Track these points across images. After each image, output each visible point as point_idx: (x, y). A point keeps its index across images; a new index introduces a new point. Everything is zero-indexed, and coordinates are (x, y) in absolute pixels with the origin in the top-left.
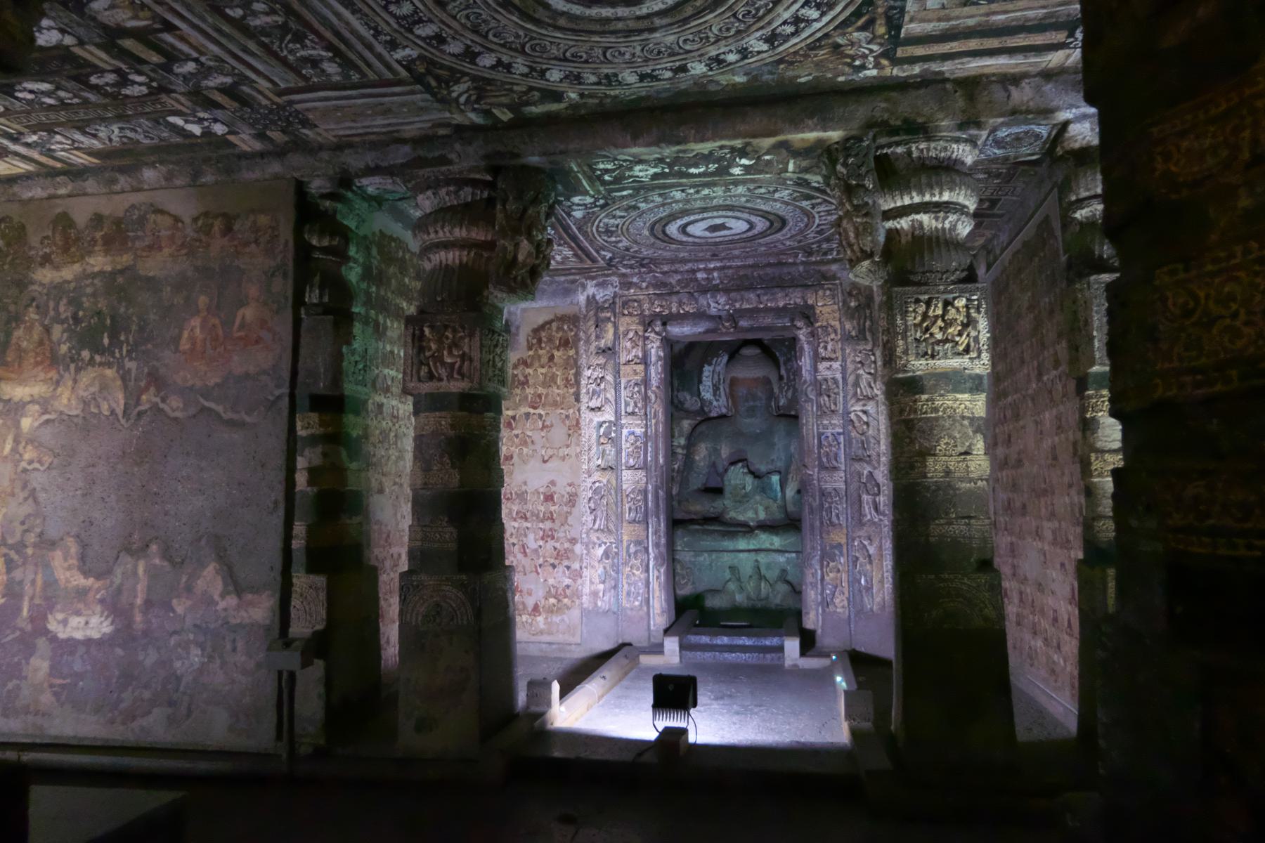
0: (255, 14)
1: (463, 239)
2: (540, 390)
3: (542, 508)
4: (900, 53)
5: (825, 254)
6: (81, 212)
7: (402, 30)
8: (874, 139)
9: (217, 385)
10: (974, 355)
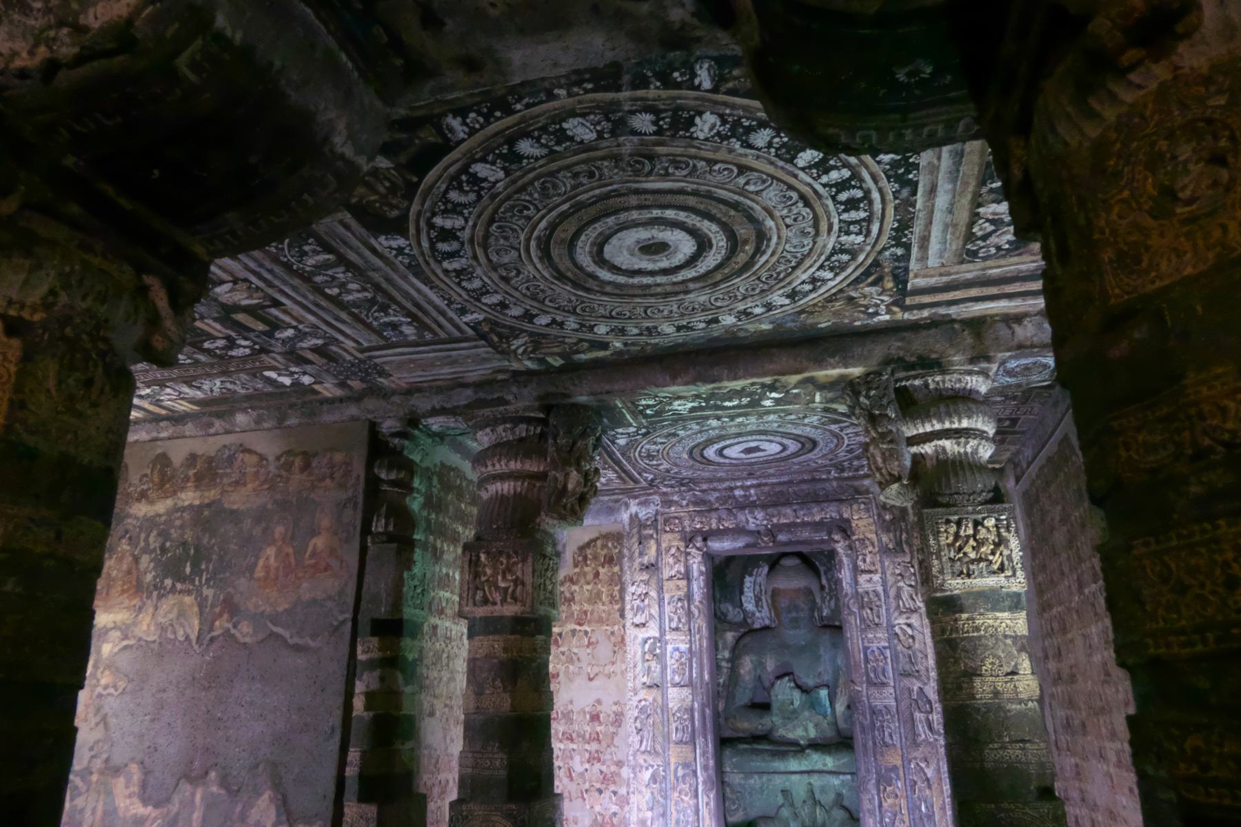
0: (349, 292)
1: (518, 471)
2: (586, 607)
3: (588, 729)
4: (908, 301)
5: (857, 470)
6: (178, 453)
8: (892, 374)
10: (1009, 573)
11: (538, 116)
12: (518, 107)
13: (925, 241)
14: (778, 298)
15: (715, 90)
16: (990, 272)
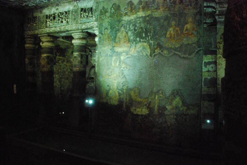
9: (179, 47)
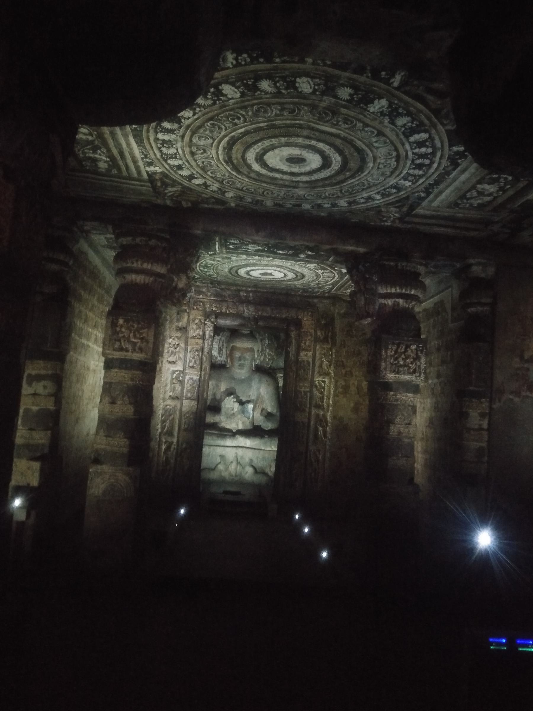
4: (407, 219)
5: (314, 293)
7: (161, 160)
11: (285, 69)
12: (278, 60)
13: (441, 193)
14: (343, 203)
15: (398, 89)
16: (458, 215)
